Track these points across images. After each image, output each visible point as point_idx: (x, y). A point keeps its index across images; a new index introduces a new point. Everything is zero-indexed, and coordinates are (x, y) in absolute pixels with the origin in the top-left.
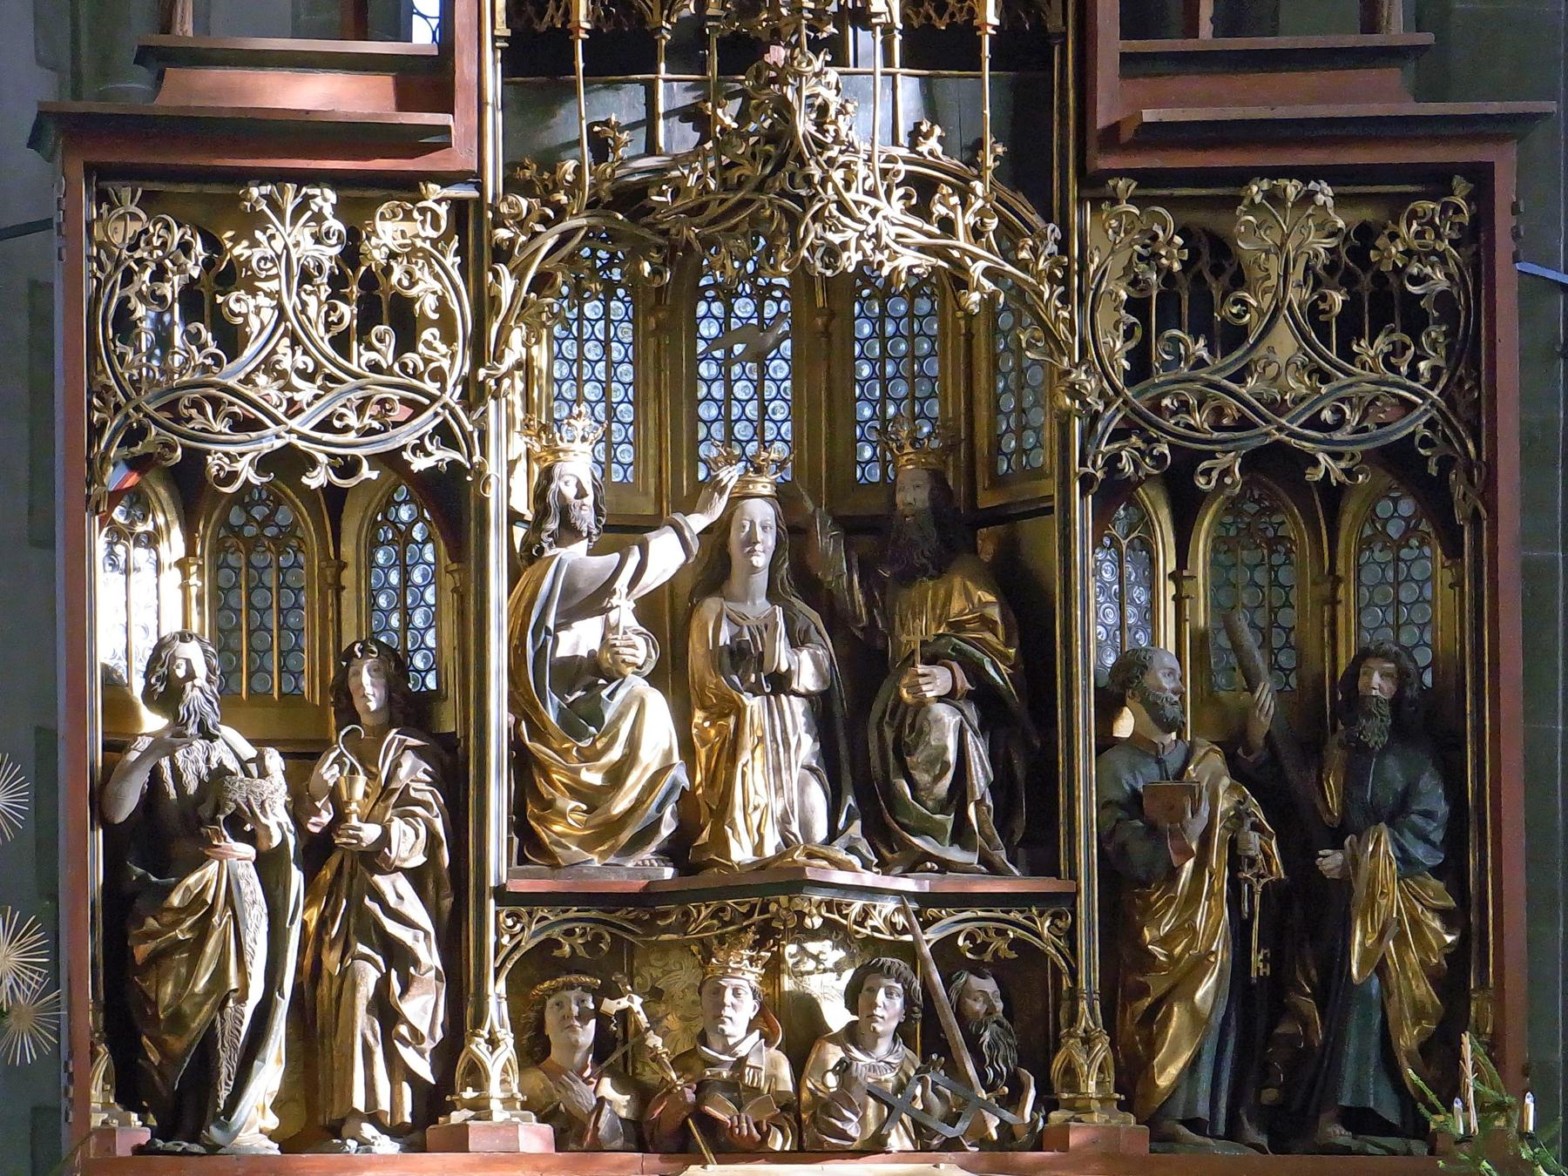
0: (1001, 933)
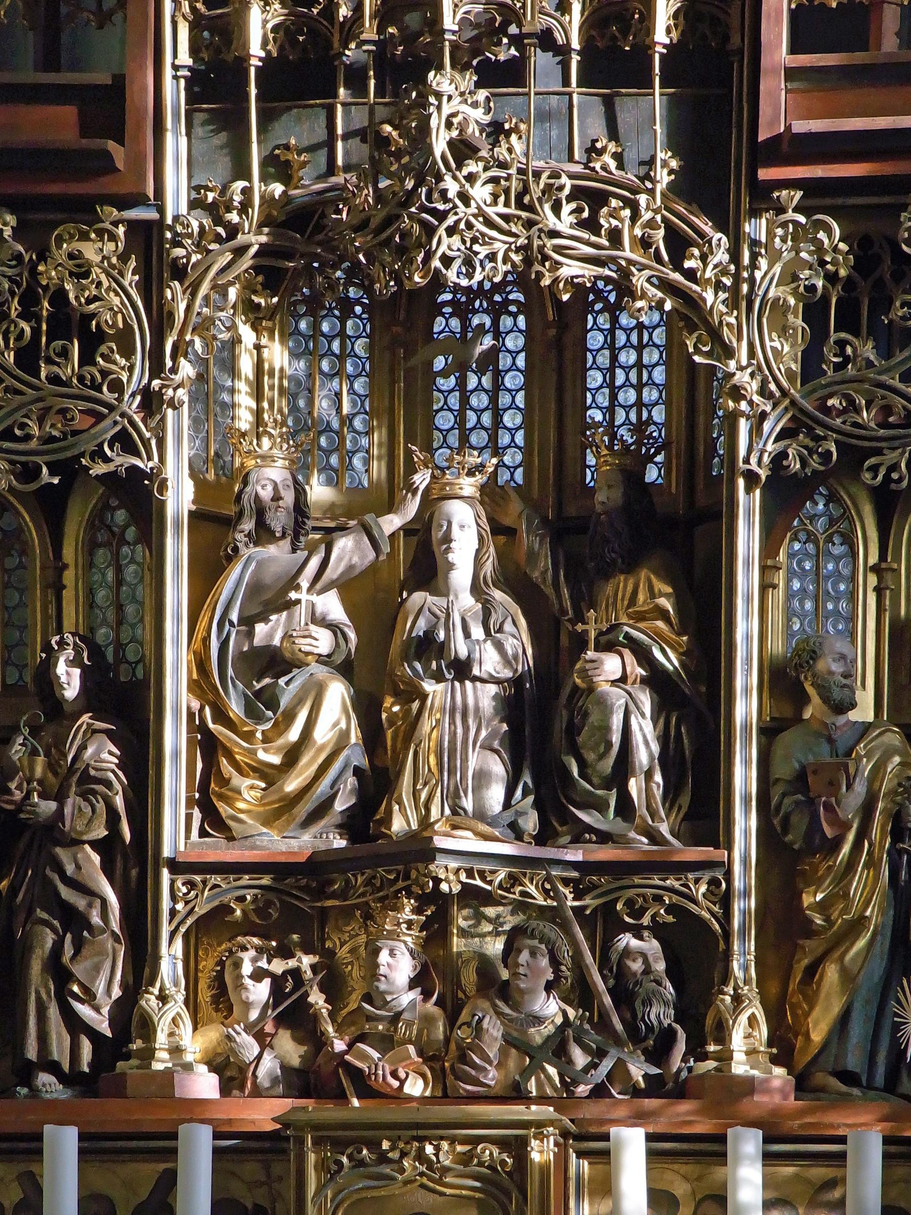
0: (658, 899)
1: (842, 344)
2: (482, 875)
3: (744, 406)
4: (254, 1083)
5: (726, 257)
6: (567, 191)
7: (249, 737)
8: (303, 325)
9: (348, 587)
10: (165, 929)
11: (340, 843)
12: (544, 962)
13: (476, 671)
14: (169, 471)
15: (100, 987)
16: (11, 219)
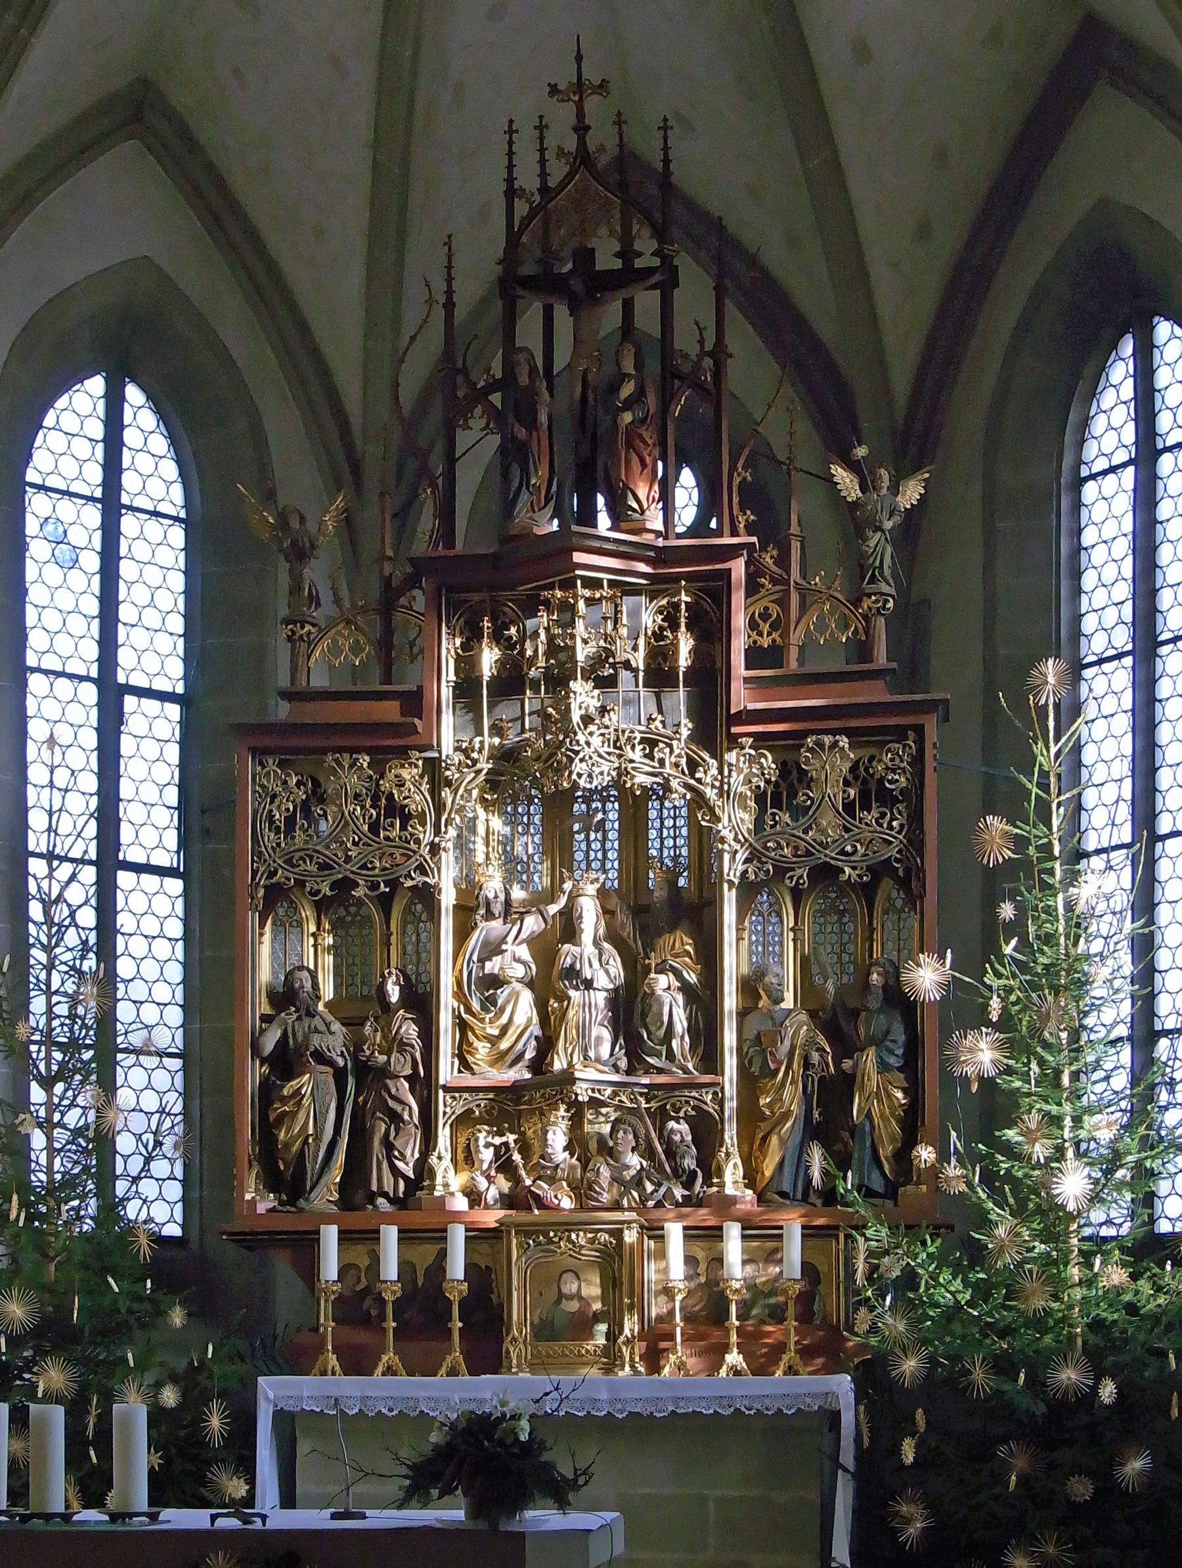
0: (687, 1102)
1: (774, 814)
2: (599, 1091)
3: (726, 847)
5: (716, 772)
6: (638, 740)
7: (482, 1021)
8: (509, 809)
9: (531, 941)
10: (441, 1122)
11: (528, 1076)
12: (631, 1137)
13: (595, 985)
14: (443, 885)
15: (408, 1153)
16: (367, 758)
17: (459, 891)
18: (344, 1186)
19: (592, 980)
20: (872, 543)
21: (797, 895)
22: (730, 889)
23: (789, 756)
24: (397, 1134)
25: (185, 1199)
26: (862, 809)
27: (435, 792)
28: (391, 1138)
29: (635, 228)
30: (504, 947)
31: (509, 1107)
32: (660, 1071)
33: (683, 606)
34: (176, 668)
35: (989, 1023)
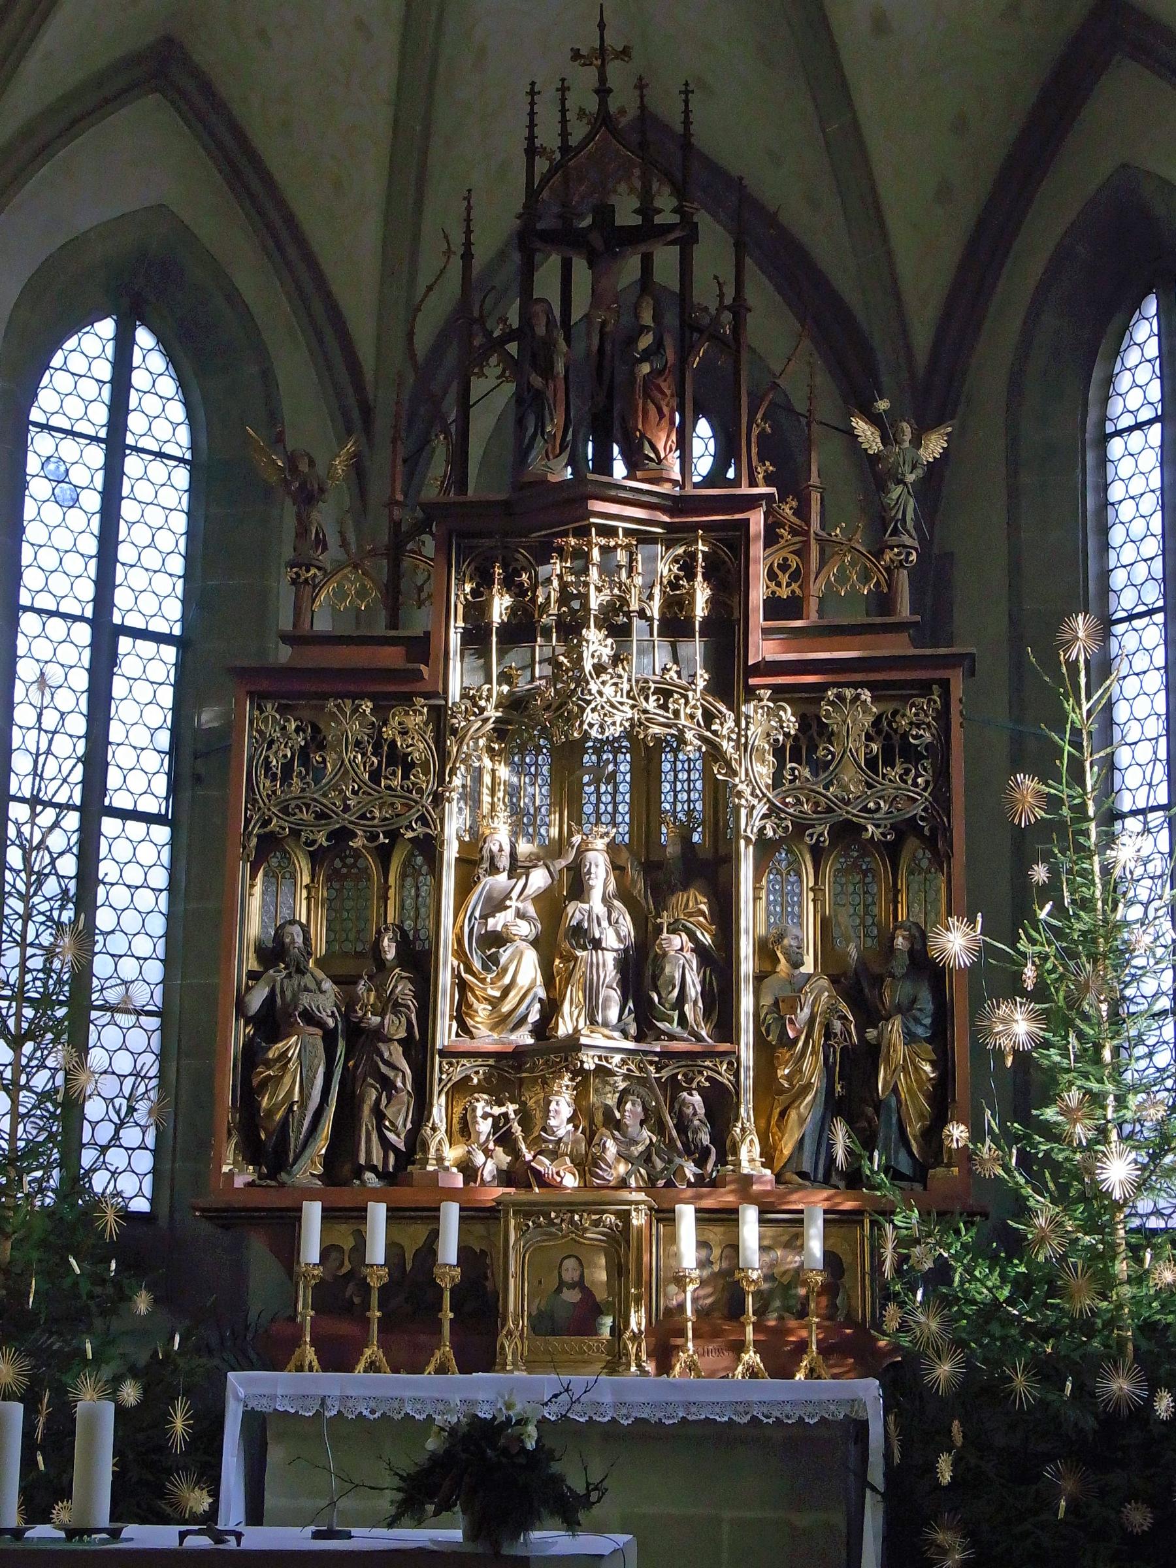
0: (701, 1073)
3: (743, 802)
4: (482, 1179)
7: (483, 981)
8: (516, 759)
10: (436, 1089)
12: (639, 1109)
13: (604, 945)
17: (462, 843)
18: (329, 1160)
19: (600, 940)
20: (895, 495)
21: (817, 853)
22: (747, 846)
23: (809, 709)
24: (389, 1102)
25: (155, 1171)
26: (885, 765)
27: (440, 741)
28: (382, 1107)
29: (655, 186)
30: (508, 903)
31: (510, 1074)
32: (672, 1037)
33: (700, 555)
34: (174, 609)
35: (1024, 993)
